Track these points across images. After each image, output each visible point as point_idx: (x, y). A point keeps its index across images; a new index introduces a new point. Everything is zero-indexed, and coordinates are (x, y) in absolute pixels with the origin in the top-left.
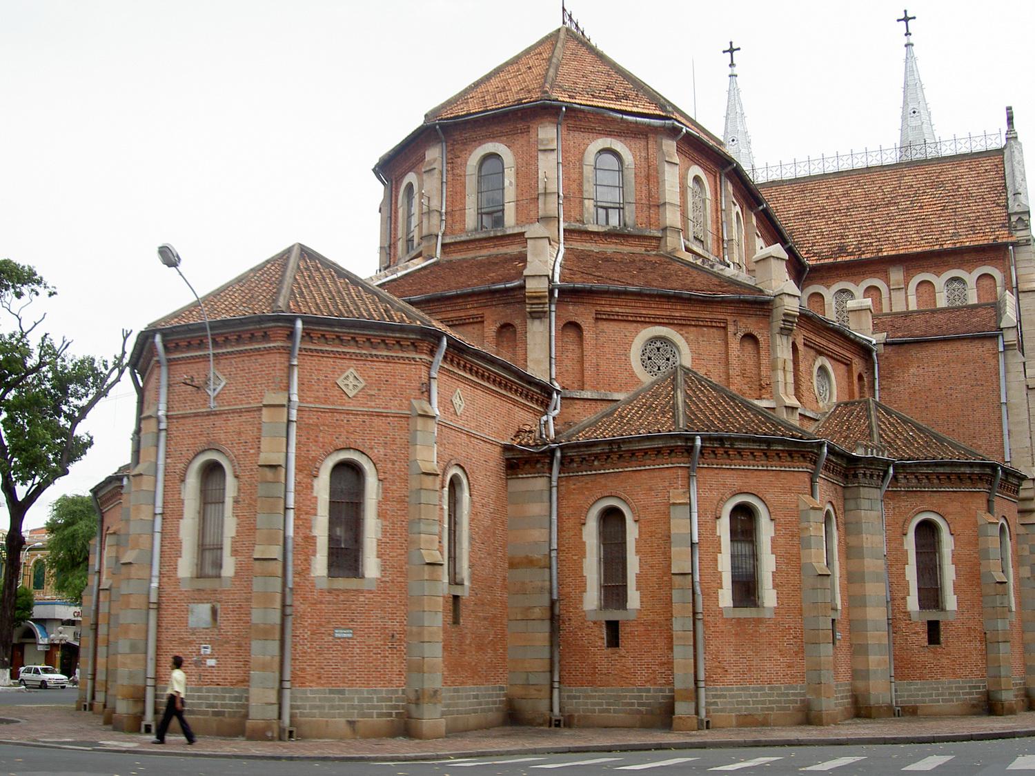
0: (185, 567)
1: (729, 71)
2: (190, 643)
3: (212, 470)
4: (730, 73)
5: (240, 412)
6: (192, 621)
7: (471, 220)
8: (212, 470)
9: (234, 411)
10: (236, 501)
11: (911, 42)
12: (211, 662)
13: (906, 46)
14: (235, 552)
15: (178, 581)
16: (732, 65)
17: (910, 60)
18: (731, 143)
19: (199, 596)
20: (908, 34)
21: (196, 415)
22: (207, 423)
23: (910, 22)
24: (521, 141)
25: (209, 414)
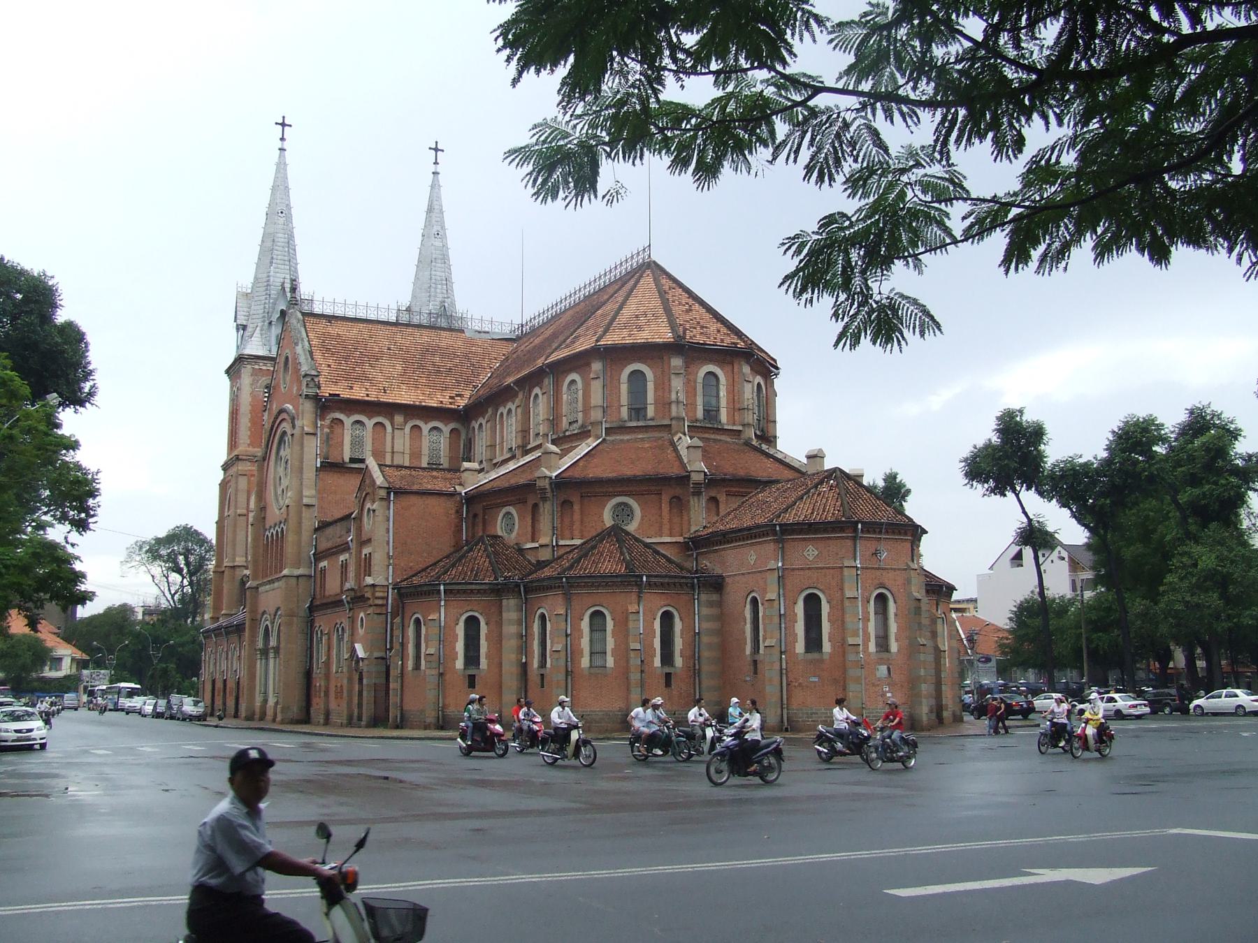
0: (872, 647)
1: (279, 144)
2: (878, 685)
3: (881, 599)
4: (280, 147)
5: (895, 569)
6: (878, 675)
7: (700, 414)
8: (881, 599)
9: (891, 569)
10: (896, 615)
11: (438, 171)
12: (889, 695)
13: (433, 173)
14: (897, 640)
15: (870, 654)
16: (282, 139)
17: (435, 186)
18: (280, 214)
19: (881, 662)
20: (436, 163)
21: (873, 568)
22: (878, 573)
23: (439, 153)
24: (729, 368)
25: (879, 569)
